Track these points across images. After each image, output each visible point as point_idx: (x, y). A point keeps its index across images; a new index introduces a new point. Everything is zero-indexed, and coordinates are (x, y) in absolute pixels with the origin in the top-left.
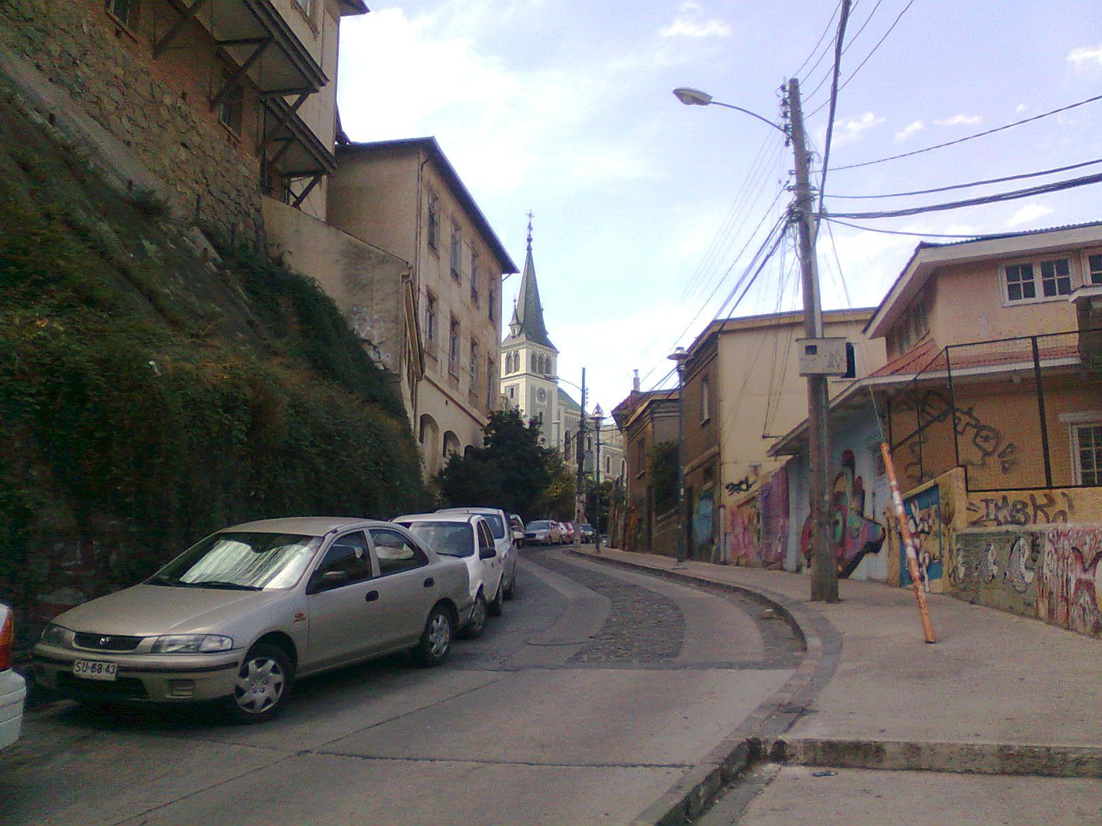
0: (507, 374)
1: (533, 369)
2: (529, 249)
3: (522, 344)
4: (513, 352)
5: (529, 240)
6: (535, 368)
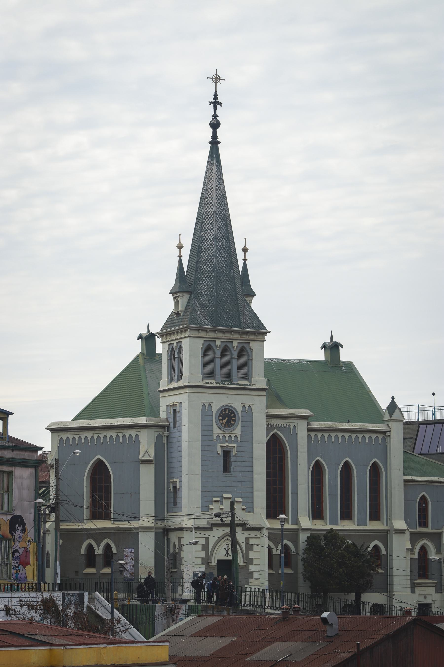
0: (171, 379)
4: (175, 344)
5: (215, 125)
6: (213, 370)
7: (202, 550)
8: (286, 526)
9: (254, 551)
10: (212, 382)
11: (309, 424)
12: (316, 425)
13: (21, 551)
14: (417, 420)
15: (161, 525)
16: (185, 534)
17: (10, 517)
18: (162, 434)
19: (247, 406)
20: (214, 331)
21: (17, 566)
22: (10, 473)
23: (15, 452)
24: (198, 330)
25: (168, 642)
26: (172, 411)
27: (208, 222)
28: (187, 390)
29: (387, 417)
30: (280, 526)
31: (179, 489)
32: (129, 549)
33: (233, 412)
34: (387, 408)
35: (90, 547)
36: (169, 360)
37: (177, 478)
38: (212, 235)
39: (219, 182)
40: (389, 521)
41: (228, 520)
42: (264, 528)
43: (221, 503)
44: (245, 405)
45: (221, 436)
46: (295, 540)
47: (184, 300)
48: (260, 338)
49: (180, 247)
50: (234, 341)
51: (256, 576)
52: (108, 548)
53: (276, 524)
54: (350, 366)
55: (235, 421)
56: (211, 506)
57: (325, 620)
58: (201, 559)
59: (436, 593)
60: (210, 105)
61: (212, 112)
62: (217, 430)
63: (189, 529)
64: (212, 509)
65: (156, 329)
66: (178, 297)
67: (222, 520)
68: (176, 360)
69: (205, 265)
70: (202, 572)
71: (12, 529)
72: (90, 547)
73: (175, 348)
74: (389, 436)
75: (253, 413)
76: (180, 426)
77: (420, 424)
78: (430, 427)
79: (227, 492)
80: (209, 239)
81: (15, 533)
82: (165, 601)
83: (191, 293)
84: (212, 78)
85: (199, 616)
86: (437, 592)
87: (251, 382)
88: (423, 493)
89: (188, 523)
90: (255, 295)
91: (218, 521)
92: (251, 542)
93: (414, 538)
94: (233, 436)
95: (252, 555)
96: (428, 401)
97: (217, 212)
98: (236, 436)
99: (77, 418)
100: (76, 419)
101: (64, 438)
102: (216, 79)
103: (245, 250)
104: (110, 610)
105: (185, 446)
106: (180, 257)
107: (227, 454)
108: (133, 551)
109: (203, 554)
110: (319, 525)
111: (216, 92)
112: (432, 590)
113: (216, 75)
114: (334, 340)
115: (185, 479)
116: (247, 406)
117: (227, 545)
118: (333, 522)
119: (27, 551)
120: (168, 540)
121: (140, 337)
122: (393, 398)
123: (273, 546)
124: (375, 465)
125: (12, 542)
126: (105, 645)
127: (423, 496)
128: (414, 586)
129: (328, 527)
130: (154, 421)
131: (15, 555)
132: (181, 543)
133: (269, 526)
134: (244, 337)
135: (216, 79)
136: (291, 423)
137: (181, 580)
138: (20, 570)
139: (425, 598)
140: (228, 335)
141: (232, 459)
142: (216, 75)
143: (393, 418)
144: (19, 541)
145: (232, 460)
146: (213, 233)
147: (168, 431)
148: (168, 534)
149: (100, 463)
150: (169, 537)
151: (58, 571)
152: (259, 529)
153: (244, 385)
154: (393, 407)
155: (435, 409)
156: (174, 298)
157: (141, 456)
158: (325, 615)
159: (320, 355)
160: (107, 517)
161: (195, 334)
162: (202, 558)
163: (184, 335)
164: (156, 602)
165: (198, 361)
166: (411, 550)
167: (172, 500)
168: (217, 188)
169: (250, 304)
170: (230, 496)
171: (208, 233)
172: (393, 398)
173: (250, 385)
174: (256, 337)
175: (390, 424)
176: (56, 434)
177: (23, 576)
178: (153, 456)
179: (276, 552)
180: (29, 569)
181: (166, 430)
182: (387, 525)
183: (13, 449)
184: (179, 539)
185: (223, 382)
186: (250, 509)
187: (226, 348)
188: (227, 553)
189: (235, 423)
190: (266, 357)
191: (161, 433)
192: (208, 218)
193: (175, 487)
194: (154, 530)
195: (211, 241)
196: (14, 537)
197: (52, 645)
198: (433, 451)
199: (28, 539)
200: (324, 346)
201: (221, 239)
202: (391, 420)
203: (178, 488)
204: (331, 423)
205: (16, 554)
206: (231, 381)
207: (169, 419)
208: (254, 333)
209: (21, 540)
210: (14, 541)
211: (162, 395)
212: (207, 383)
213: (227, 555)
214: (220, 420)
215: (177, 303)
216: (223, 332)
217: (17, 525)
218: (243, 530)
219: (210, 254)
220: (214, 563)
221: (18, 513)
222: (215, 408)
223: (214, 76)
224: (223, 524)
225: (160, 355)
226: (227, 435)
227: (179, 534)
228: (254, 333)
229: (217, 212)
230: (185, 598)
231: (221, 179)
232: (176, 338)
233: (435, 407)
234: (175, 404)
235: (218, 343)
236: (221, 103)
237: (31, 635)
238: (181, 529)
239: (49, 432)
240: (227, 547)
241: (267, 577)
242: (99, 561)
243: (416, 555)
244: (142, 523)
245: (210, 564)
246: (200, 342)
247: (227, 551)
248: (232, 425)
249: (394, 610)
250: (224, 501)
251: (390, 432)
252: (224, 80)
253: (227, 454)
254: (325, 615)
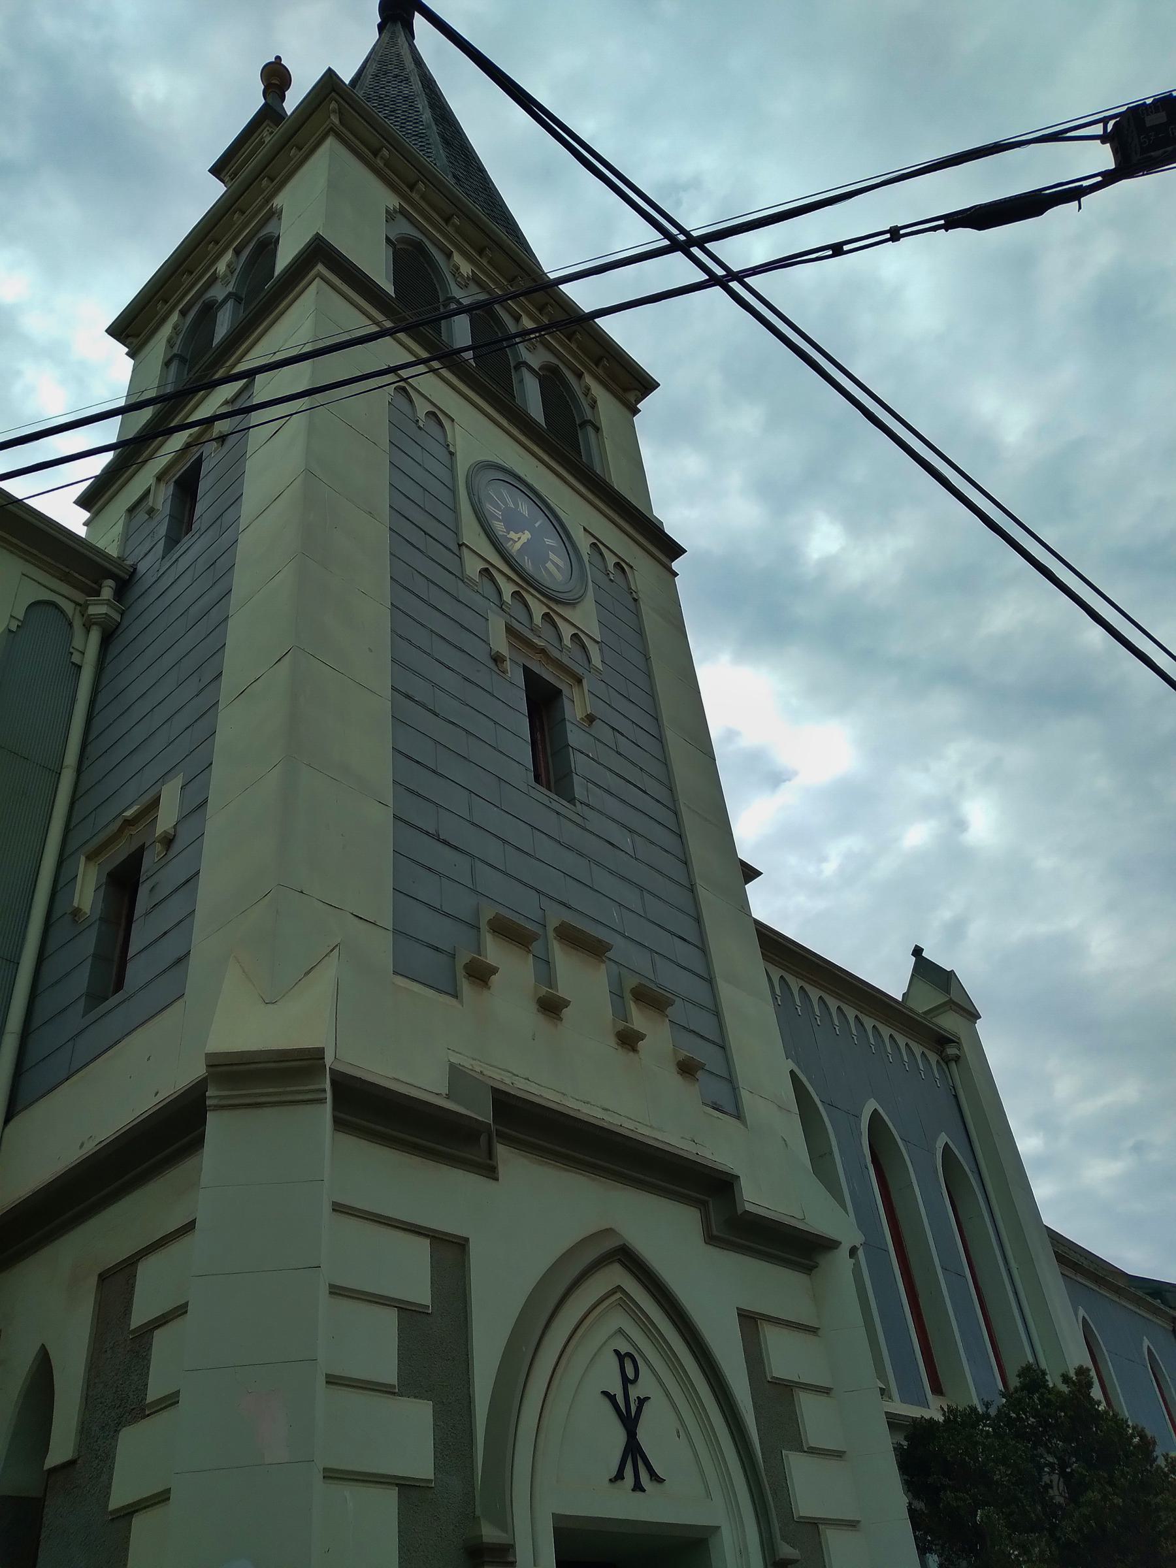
9: (813, 1451)
18: (70, 615)
31: (168, 841)
58: (389, 1498)
74: (957, 1059)
75: (635, 600)
117: (621, 1357)
122: (917, 952)
141: (575, 737)
172: (917, 952)
181: (107, 592)
188: (633, 1450)
191: (68, 607)
218: (715, 1233)
240: (626, 1382)
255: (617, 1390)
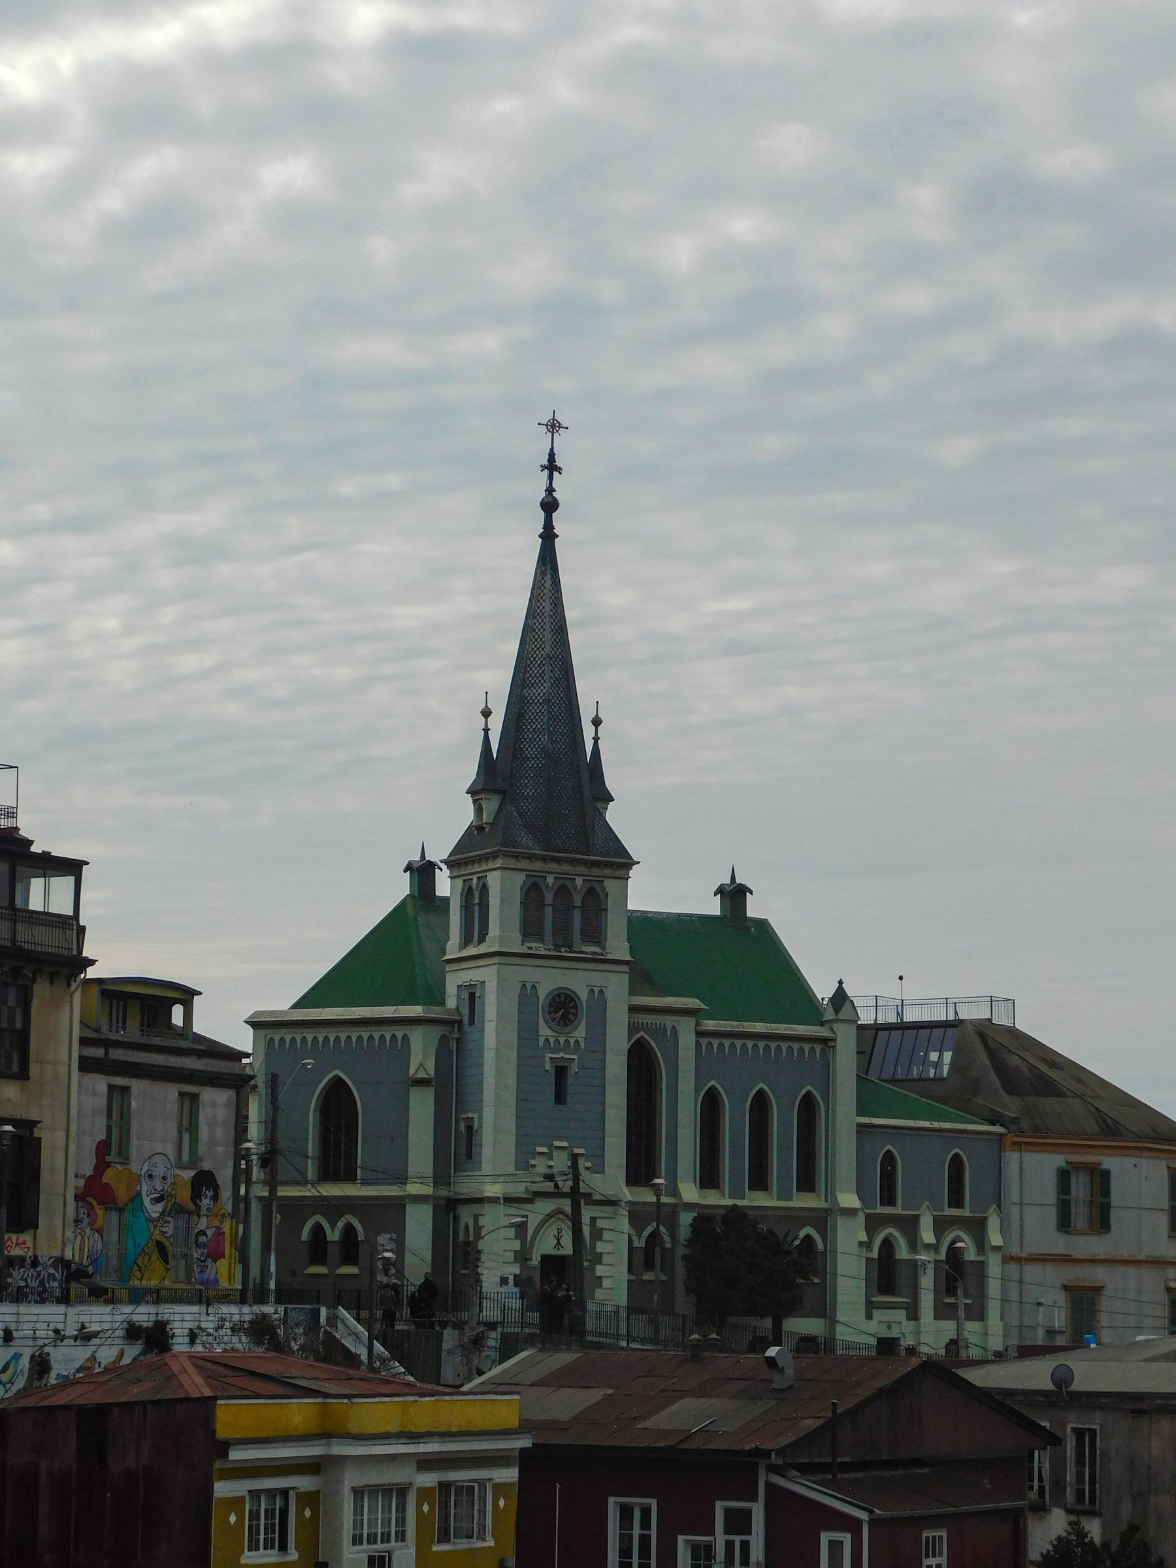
0: (466, 941)
1: (531, 929)
2: (548, 536)
3: (494, 856)
4: (475, 881)
5: (550, 505)
7: (516, 1238)
8: (664, 1199)
10: (539, 948)
11: (698, 1024)
12: (710, 1025)
13: (210, 1233)
14: (872, 1022)
15: (443, 1193)
16: (487, 1209)
17: (192, 1173)
19: (597, 990)
20: (544, 859)
21: (202, 1259)
22: (194, 1098)
23: (204, 1061)
24: (516, 856)
25: (518, 1393)
26: (467, 996)
27: (536, 672)
28: (496, 960)
29: (829, 1015)
30: (653, 1199)
31: (477, 1131)
32: (387, 1232)
33: (572, 1000)
34: (831, 999)
35: (318, 1229)
36: (464, 908)
37: (474, 1111)
38: (542, 694)
39: (555, 604)
40: (830, 1194)
41: (567, 1186)
42: (622, 1201)
43: (549, 1156)
44: (594, 988)
45: (552, 1040)
46: (672, 1223)
47: (491, 805)
48: (620, 873)
49: (486, 713)
50: (577, 878)
51: (606, 1283)
52: (349, 1230)
53: (648, 1197)
54: (763, 926)
55: (575, 1015)
56: (532, 1162)
57: (771, 1362)
58: (513, 1252)
59: (907, 1320)
60: (542, 471)
61: (544, 484)
62: (544, 1031)
63: (493, 1200)
64: (533, 1166)
65: (439, 852)
66: (481, 799)
67: (556, 1186)
68: (477, 908)
69: (529, 746)
70: (515, 1276)
71: (196, 1195)
72: (318, 1229)
73: (474, 887)
74: (834, 1047)
76: (482, 1021)
77: (877, 1028)
78: (896, 1034)
79: (561, 1138)
80: (536, 701)
81: (201, 1201)
82: (459, 1326)
83: (503, 793)
84: (547, 425)
85: (542, 1350)
86: (909, 1319)
87: (603, 948)
88: (889, 1147)
89: (493, 1190)
90: (611, 799)
91: (549, 1186)
92: (600, 1224)
93: (873, 1223)
94: (572, 1041)
95: (600, 1247)
96: (891, 991)
97: (551, 656)
98: (577, 1041)
99: (299, 1005)
100: (297, 1006)
101: (277, 1038)
102: (554, 426)
103: (597, 722)
104: (365, 1340)
105: (489, 1056)
106: (486, 730)
107: (561, 1072)
108: (394, 1236)
109: (516, 1245)
110: (714, 1198)
111: (552, 449)
112: (900, 1315)
113: (554, 419)
114: (738, 882)
115: (488, 1114)
116: (597, 990)
118: (736, 1193)
119: (219, 1234)
120: (456, 1219)
121: (409, 868)
122: (841, 982)
123: (633, 1232)
124: (808, 1097)
125: (196, 1217)
126: (416, 1398)
127: (889, 1152)
128: (870, 1307)
129: (729, 1202)
130: (435, 1012)
131: (200, 1241)
132: (480, 1225)
133: (630, 1199)
134: (595, 871)
135: (553, 426)
136: (669, 1021)
137: (479, 1288)
138: (207, 1267)
139: (889, 1327)
140: (566, 868)
141: (570, 1080)
142: (554, 419)
143: (840, 1016)
144: (207, 1216)
145: (569, 1082)
146: (544, 691)
147: (458, 1031)
148: (455, 1210)
149: (338, 1083)
150: (457, 1214)
151: (273, 1269)
152: (613, 1203)
153: (593, 953)
154: (840, 998)
155: (902, 1003)
156: (475, 801)
157: (411, 1072)
158: (772, 1351)
159: (713, 907)
160: (349, 1176)
161: (512, 863)
162: (515, 1251)
163: (491, 865)
164: (444, 1325)
165: (516, 910)
166: (867, 1245)
167: (463, 1151)
168: (552, 614)
169: (604, 815)
170: (565, 1144)
171: (534, 691)
172: (841, 982)
173: (602, 954)
174: (614, 872)
175: (836, 1027)
176: (262, 1032)
177: (212, 1276)
178: (432, 1073)
179: (640, 1243)
180: (223, 1264)
181: (456, 1028)
182: (826, 1200)
183: (200, 1054)
184: (476, 1217)
185: (557, 947)
186: (599, 1168)
187: (563, 890)
188: (558, 1243)
189: (575, 1019)
190: (632, 905)
191: (447, 1034)
192: (536, 666)
193: (470, 1128)
194: (432, 1200)
195: (541, 704)
196: (199, 1208)
197: (327, 1395)
198: (900, 1074)
199: (222, 1212)
200: (720, 891)
201: (557, 702)
202: (836, 1021)
203: (475, 1127)
204: (735, 1023)
205: (202, 1239)
206: (570, 946)
207: (461, 1010)
208: (611, 865)
209: (210, 1214)
210: (199, 1216)
211: (448, 967)
212: (530, 948)
213: (557, 1247)
214: (550, 1013)
215: (479, 810)
216: (558, 861)
217: (204, 1187)
219: (539, 726)
220: (536, 1261)
221: (207, 1166)
222: (543, 993)
223: (549, 421)
224: (557, 1194)
225: (446, 901)
226: (562, 1040)
227: (475, 1208)
228: (611, 865)
229: (551, 656)
230: (495, 1320)
231: (559, 598)
232: (477, 869)
233: (902, 1000)
234: (472, 983)
235: (550, 880)
236: (560, 469)
237: (287, 1377)
238: (480, 1201)
239: (250, 1030)
240: (559, 1233)
241: (626, 1285)
242: (334, 1253)
243: (875, 1254)
244: (412, 1189)
245: (528, 1262)
246: (519, 879)
247: (558, 1240)
248: (572, 1022)
249: (838, 1348)
250: (555, 1153)
251: (834, 1040)
252: (567, 428)
253: (561, 1072)
254: (772, 1351)
255: (556, 1234)
